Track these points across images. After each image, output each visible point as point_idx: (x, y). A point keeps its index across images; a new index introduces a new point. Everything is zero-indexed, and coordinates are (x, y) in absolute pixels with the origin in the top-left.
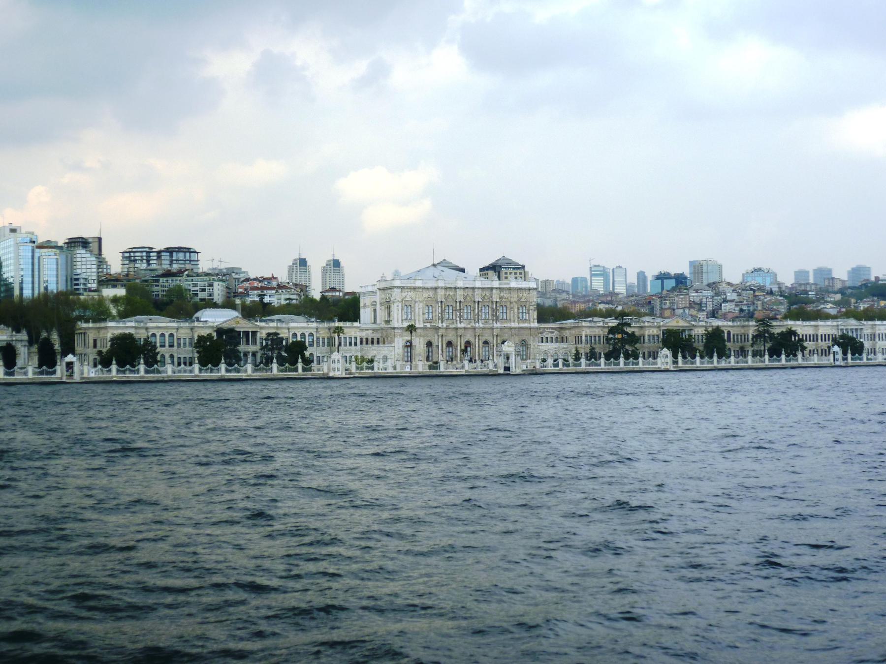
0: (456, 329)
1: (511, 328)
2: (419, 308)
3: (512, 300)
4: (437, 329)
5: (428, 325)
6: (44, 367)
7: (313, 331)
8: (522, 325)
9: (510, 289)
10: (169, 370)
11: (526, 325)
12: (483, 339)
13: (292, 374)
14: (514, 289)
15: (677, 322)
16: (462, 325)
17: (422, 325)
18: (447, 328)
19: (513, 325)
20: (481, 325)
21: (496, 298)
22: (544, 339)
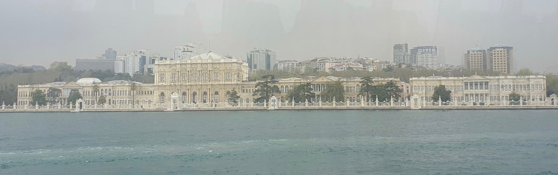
0: (186, 86)
1: (220, 85)
2: (168, 76)
3: (221, 69)
4: (175, 85)
5: (173, 84)
6: (513, 100)
7: (111, 88)
8: (226, 83)
9: (220, 63)
10: (348, 104)
11: (229, 83)
12: (203, 91)
13: (516, 106)
14: (222, 63)
15: (323, 79)
16: (190, 84)
17: (169, 84)
18: (181, 86)
19: (221, 83)
20: (200, 84)
21: (210, 68)
22: (245, 91)
